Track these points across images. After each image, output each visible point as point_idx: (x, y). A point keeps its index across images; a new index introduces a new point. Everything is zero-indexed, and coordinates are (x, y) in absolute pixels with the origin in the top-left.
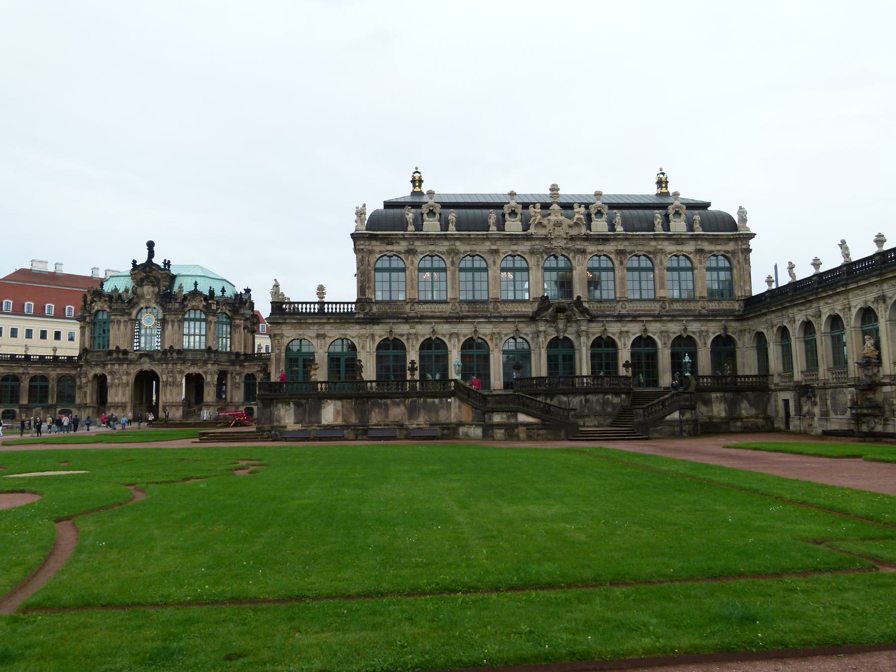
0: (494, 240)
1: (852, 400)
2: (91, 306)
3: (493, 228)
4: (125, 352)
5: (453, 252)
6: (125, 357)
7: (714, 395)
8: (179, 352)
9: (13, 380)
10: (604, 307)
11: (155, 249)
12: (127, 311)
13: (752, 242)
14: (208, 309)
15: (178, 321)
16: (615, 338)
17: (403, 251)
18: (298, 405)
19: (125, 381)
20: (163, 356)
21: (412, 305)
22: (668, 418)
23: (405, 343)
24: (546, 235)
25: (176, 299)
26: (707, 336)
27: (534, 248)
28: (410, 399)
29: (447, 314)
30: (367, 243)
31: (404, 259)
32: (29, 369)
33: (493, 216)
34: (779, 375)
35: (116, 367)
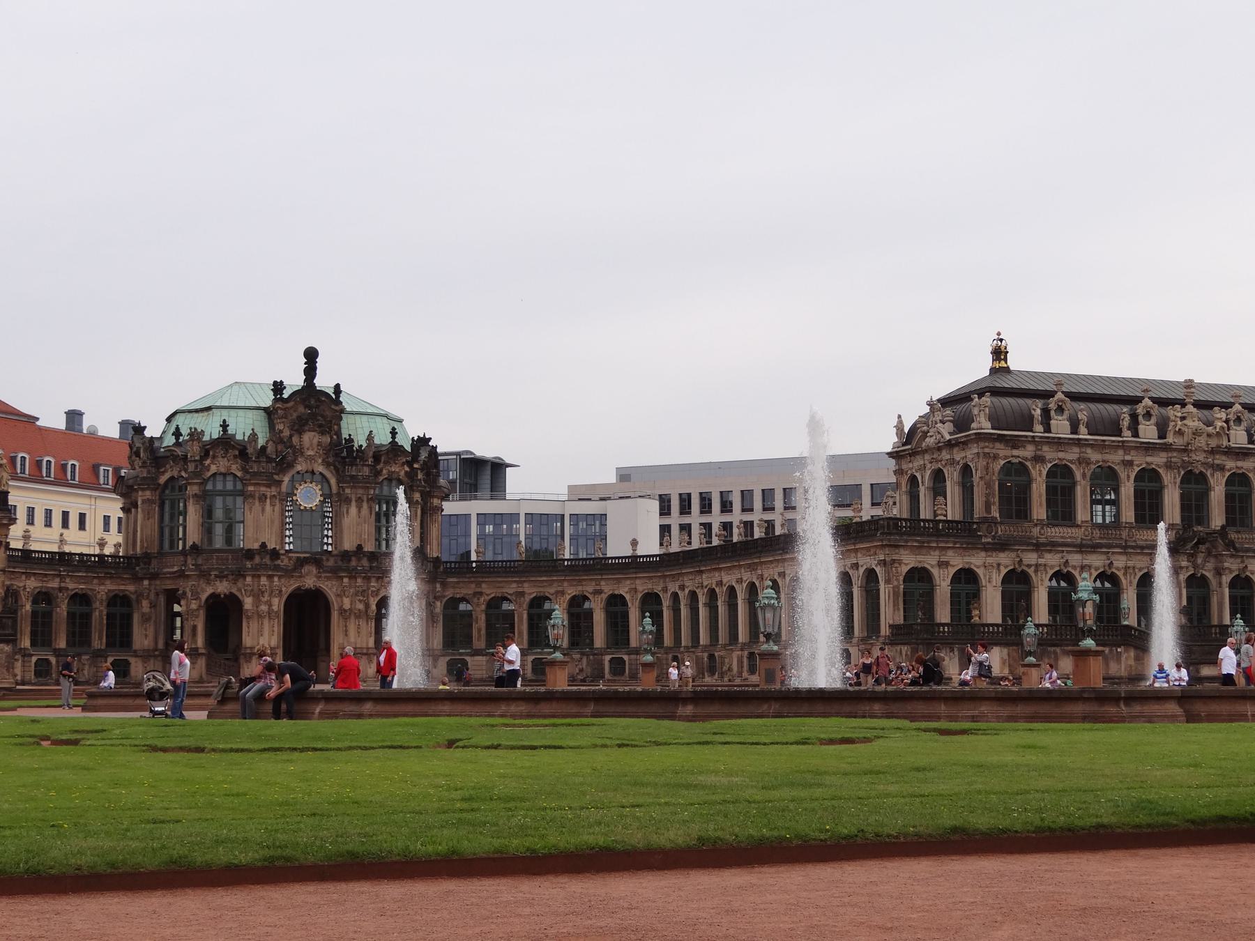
0: (1123, 446)
2: (203, 465)
3: (1127, 434)
4: (275, 554)
5: (1083, 461)
6: (277, 563)
10: (1242, 538)
12: (276, 477)
15: (368, 500)
17: (1029, 457)
20: (340, 563)
21: (1042, 528)
23: (1033, 575)
24: (1185, 446)
25: (366, 461)
27: (1171, 461)
30: (991, 446)
31: (1030, 468)
32: (68, 580)
35: (264, 580)
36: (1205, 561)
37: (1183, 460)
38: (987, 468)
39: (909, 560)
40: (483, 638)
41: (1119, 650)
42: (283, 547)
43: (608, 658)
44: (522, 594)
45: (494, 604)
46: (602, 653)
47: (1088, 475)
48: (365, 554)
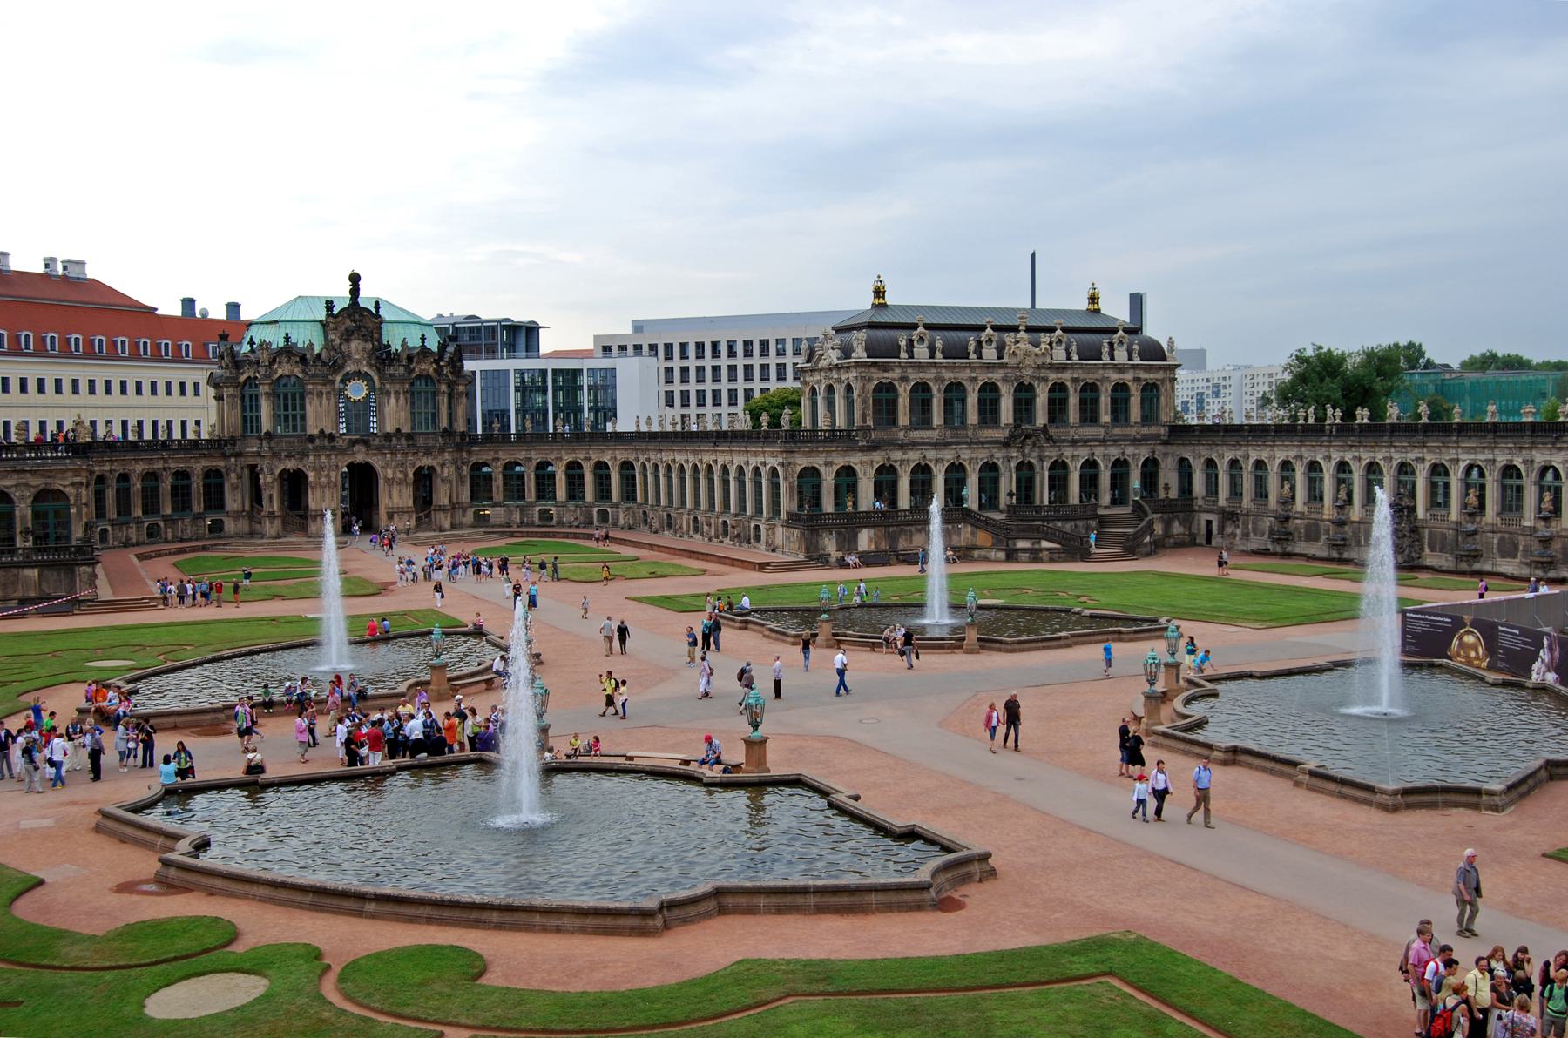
1: (1270, 527)
3: (972, 356)
4: (331, 438)
5: (938, 379)
8: (409, 437)
11: (362, 284)
12: (330, 377)
16: (1068, 461)
18: (839, 533)
19: (333, 479)
20: (384, 442)
23: (898, 467)
26: (1139, 458)
33: (971, 339)
34: (1203, 498)
35: (323, 459)
36: (1031, 450)
38: (863, 388)
39: (802, 462)
40: (501, 493)
42: (338, 431)
43: (596, 509)
44: (530, 459)
45: (510, 466)
47: (943, 389)
48: (402, 435)
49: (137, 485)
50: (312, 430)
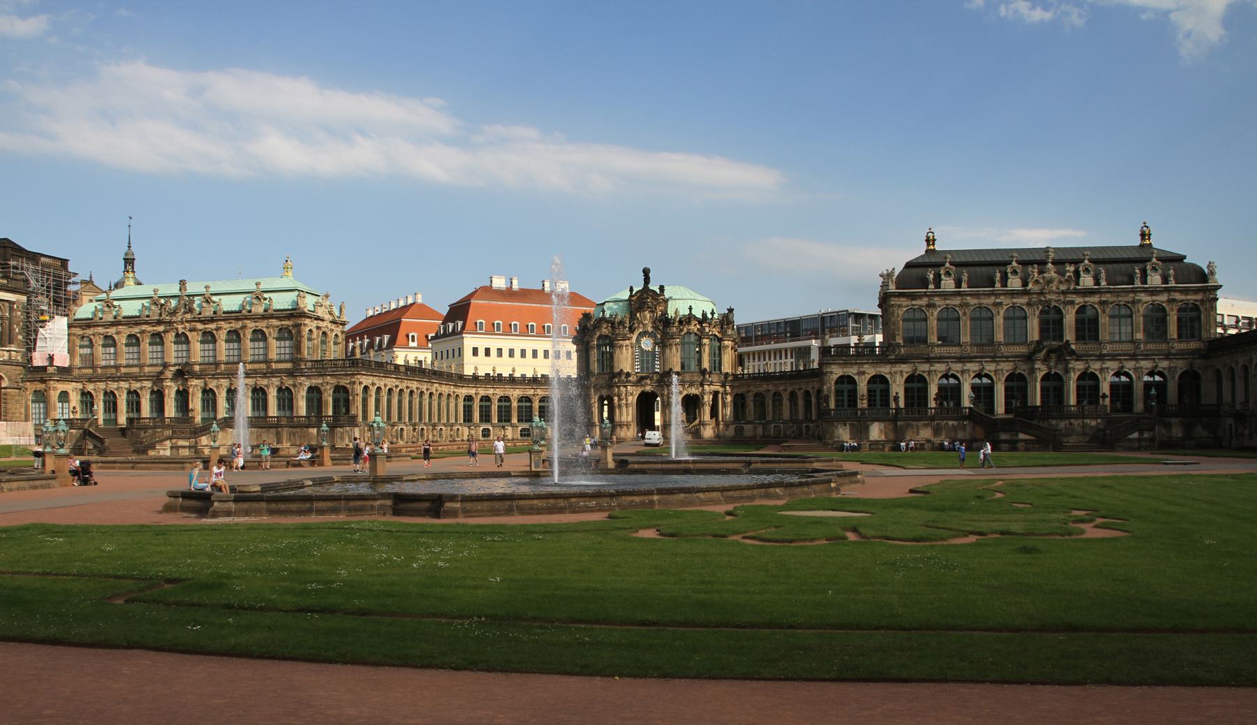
3: (998, 285)
4: (628, 375)
7: (1173, 420)
9: (526, 401)
11: (651, 275)
12: (628, 336)
13: (1219, 293)
14: (702, 332)
16: (1097, 373)
18: (851, 425)
22: (1131, 437)
25: (674, 323)
26: (1177, 372)
28: (936, 422)
29: (959, 356)
30: (896, 299)
32: (538, 390)
36: (1056, 363)
37: (1041, 300)
41: (965, 423)
43: (804, 425)
46: (802, 422)
49: (515, 404)
50: (616, 370)
